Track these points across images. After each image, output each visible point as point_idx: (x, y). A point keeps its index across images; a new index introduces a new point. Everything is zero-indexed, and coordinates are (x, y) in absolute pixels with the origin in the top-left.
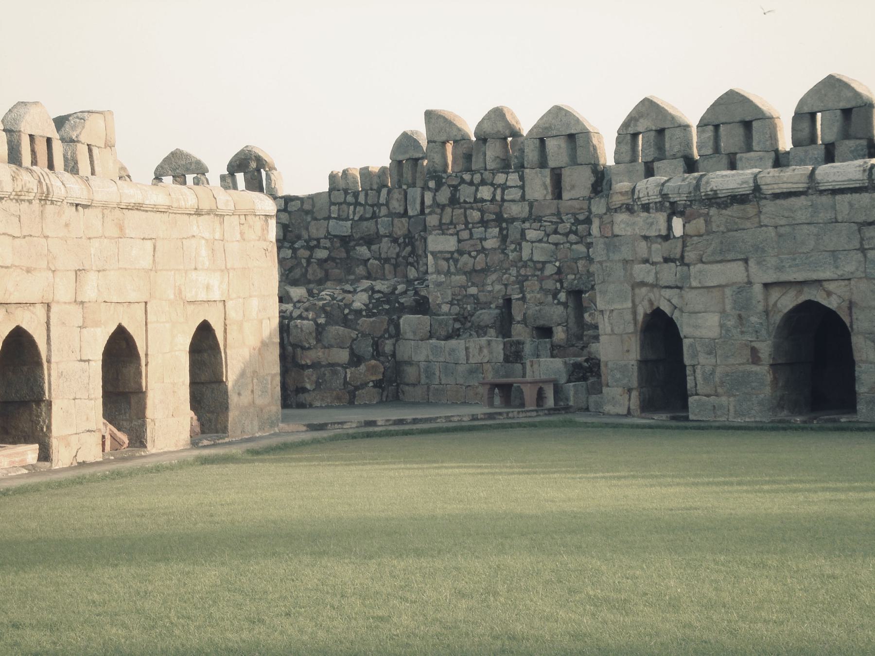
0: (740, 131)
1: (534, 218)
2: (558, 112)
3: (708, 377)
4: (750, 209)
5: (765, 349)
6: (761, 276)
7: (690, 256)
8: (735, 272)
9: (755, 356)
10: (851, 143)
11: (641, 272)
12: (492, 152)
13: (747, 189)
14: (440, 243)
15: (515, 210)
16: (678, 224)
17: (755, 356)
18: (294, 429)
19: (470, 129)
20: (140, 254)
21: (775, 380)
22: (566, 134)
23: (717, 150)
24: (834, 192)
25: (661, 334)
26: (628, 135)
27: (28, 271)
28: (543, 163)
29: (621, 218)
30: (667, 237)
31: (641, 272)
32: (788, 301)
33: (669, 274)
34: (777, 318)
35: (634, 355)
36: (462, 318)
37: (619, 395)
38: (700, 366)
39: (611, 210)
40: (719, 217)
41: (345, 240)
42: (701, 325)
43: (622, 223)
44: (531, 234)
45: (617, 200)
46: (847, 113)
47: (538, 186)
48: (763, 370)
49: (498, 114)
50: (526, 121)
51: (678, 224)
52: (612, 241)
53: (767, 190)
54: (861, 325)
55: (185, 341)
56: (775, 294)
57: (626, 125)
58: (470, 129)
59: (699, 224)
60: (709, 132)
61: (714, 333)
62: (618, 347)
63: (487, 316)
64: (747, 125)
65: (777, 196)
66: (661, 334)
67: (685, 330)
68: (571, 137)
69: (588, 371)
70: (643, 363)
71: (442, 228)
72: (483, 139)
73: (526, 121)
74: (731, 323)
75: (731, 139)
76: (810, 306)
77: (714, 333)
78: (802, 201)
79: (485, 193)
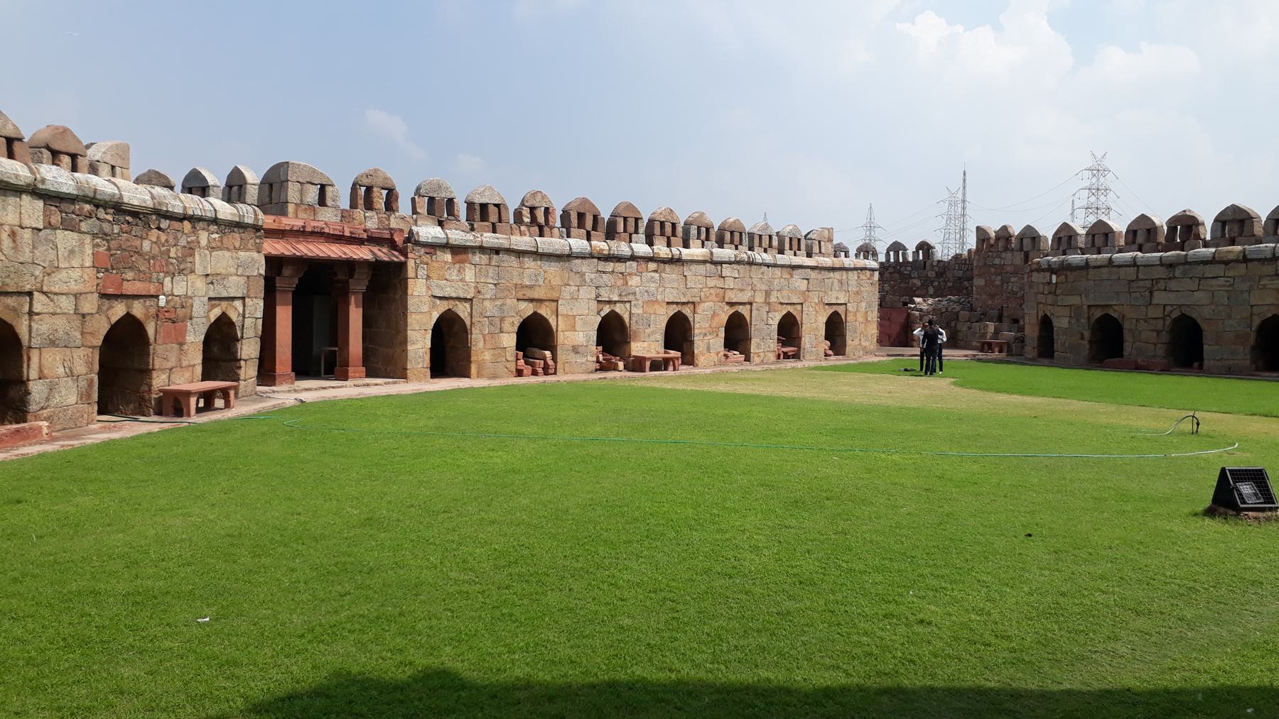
0: (1102, 238)
1: (1015, 273)
2: (1029, 228)
3: (1063, 344)
4: (1084, 273)
5: (1087, 334)
6: (1086, 303)
7: (1058, 292)
8: (1075, 300)
9: (1082, 338)
10: (1150, 244)
11: (1041, 298)
12: (1001, 244)
13: (1083, 263)
14: (979, 282)
15: (1008, 269)
16: (1054, 277)
17: (1082, 338)
18: (881, 358)
19: (993, 235)
20: (803, 285)
21: (1091, 347)
22: (1030, 235)
23: (1093, 245)
24: (1119, 266)
25: (1046, 324)
26: (1058, 238)
27: (742, 290)
28: (1021, 249)
29: (1035, 274)
30: (1050, 283)
31: (1041, 298)
32: (1098, 314)
33: (1050, 299)
34: (1093, 320)
35: (1036, 334)
36: (984, 314)
37: (1030, 351)
38: (1060, 340)
39: (1032, 271)
40: (1071, 276)
41: (960, 278)
42: (1061, 323)
43: (1036, 277)
44: (1013, 279)
45: (1034, 267)
46: (1149, 230)
47: (1018, 259)
48: (1086, 343)
49: (1005, 228)
50: (1016, 230)
51: (1054, 277)
52: (1031, 284)
53: (1091, 264)
54: (1126, 325)
55: (823, 319)
56: (1093, 310)
57: (1056, 234)
58: (993, 235)
59: (1063, 278)
60: (1131, 236)
61: (1066, 325)
62: (1032, 331)
63: (995, 313)
64: (1106, 235)
65: (1095, 267)
66: (1046, 324)
67: (1055, 324)
68: (1033, 239)
69: (1022, 340)
70: (1040, 338)
71: (980, 276)
72: (998, 238)
73: (1016, 230)
74: (1073, 321)
75: (1099, 241)
76: (1107, 315)
77: (1066, 325)
78: (1105, 270)
79: (997, 261)
